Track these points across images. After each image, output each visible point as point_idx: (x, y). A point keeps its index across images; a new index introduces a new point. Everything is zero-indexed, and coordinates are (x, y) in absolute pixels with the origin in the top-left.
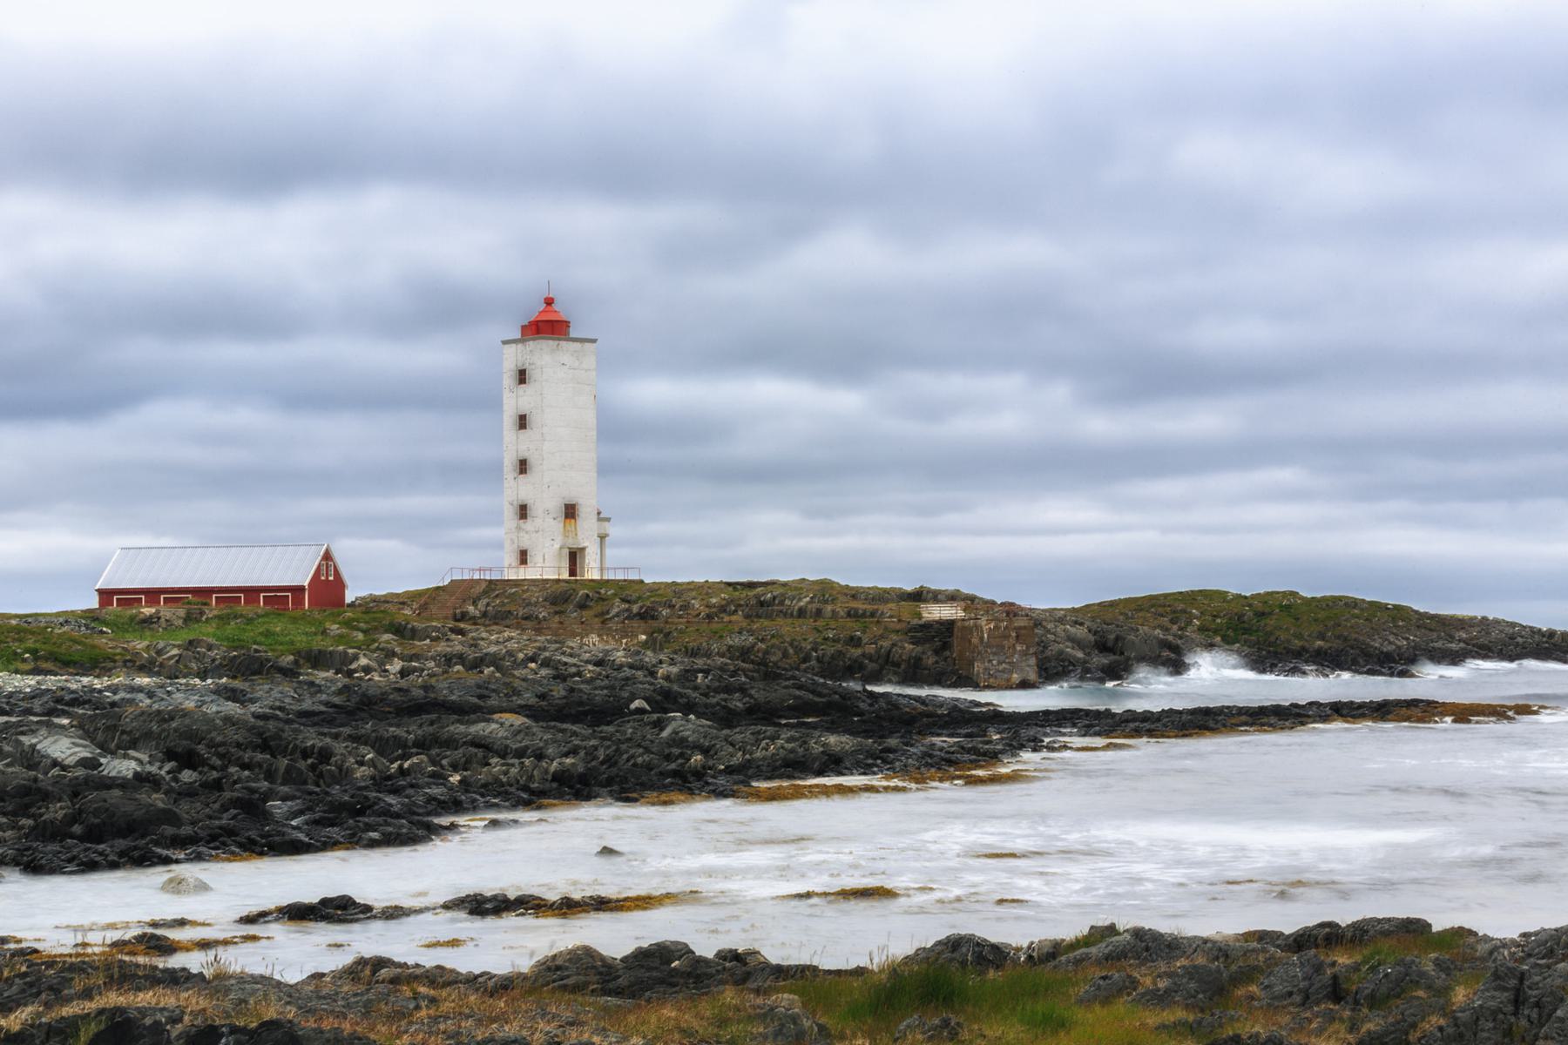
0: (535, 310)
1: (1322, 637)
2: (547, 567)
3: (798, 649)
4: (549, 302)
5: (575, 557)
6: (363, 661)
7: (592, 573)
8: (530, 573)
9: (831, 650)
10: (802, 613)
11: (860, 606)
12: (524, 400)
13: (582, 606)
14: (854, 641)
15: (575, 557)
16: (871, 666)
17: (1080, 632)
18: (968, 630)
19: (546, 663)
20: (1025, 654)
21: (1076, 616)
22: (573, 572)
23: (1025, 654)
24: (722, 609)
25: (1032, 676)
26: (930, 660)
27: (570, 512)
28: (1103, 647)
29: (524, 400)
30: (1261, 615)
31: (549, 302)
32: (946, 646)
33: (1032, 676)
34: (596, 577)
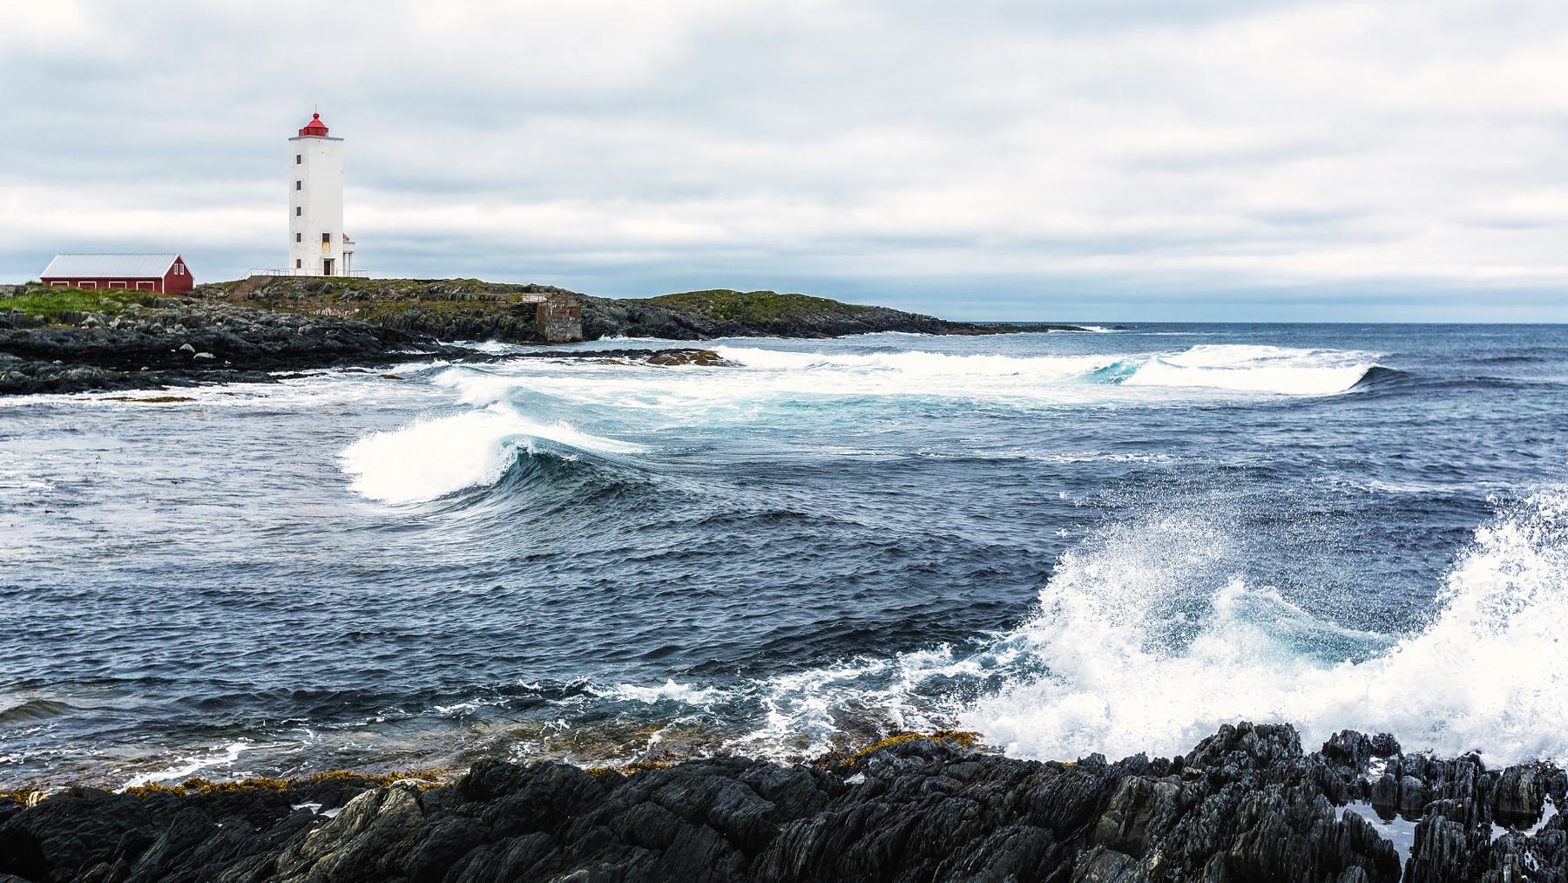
0: (307, 121)
1: (779, 316)
2: (313, 269)
3: (445, 318)
4: (316, 116)
5: (328, 264)
6: (90, 319)
7: (338, 271)
8: (300, 273)
9: (464, 319)
10: (453, 297)
11: (487, 294)
12: (299, 172)
13: (327, 292)
14: (479, 314)
15: (328, 264)
16: (487, 328)
17: (620, 311)
18: (543, 308)
19: (229, 323)
20: (574, 322)
21: (621, 303)
22: (327, 272)
23: (574, 322)
24: (408, 295)
25: (579, 335)
26: (521, 326)
27: (326, 238)
28: (631, 319)
29: (299, 172)
30: (747, 304)
31: (316, 116)
32: (532, 318)
33: (579, 335)
34: (340, 275)
